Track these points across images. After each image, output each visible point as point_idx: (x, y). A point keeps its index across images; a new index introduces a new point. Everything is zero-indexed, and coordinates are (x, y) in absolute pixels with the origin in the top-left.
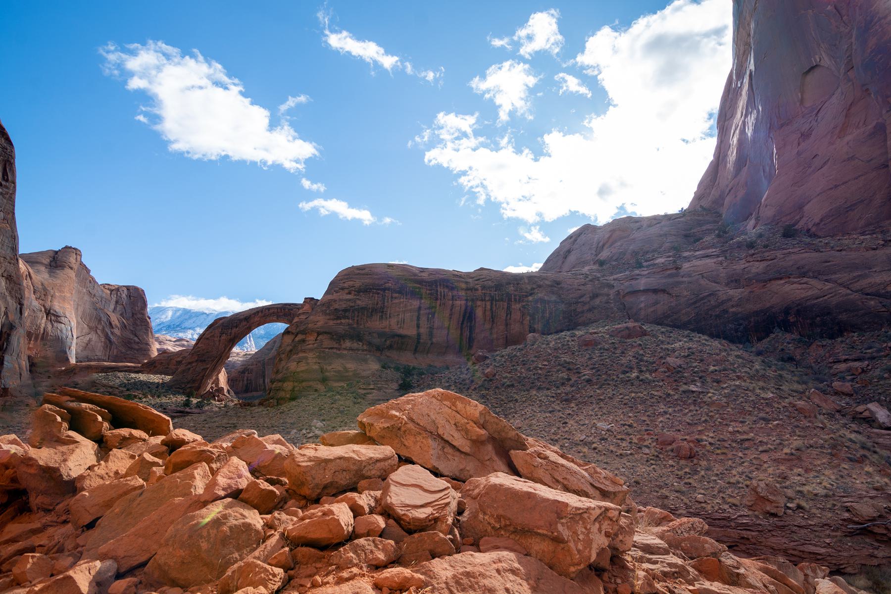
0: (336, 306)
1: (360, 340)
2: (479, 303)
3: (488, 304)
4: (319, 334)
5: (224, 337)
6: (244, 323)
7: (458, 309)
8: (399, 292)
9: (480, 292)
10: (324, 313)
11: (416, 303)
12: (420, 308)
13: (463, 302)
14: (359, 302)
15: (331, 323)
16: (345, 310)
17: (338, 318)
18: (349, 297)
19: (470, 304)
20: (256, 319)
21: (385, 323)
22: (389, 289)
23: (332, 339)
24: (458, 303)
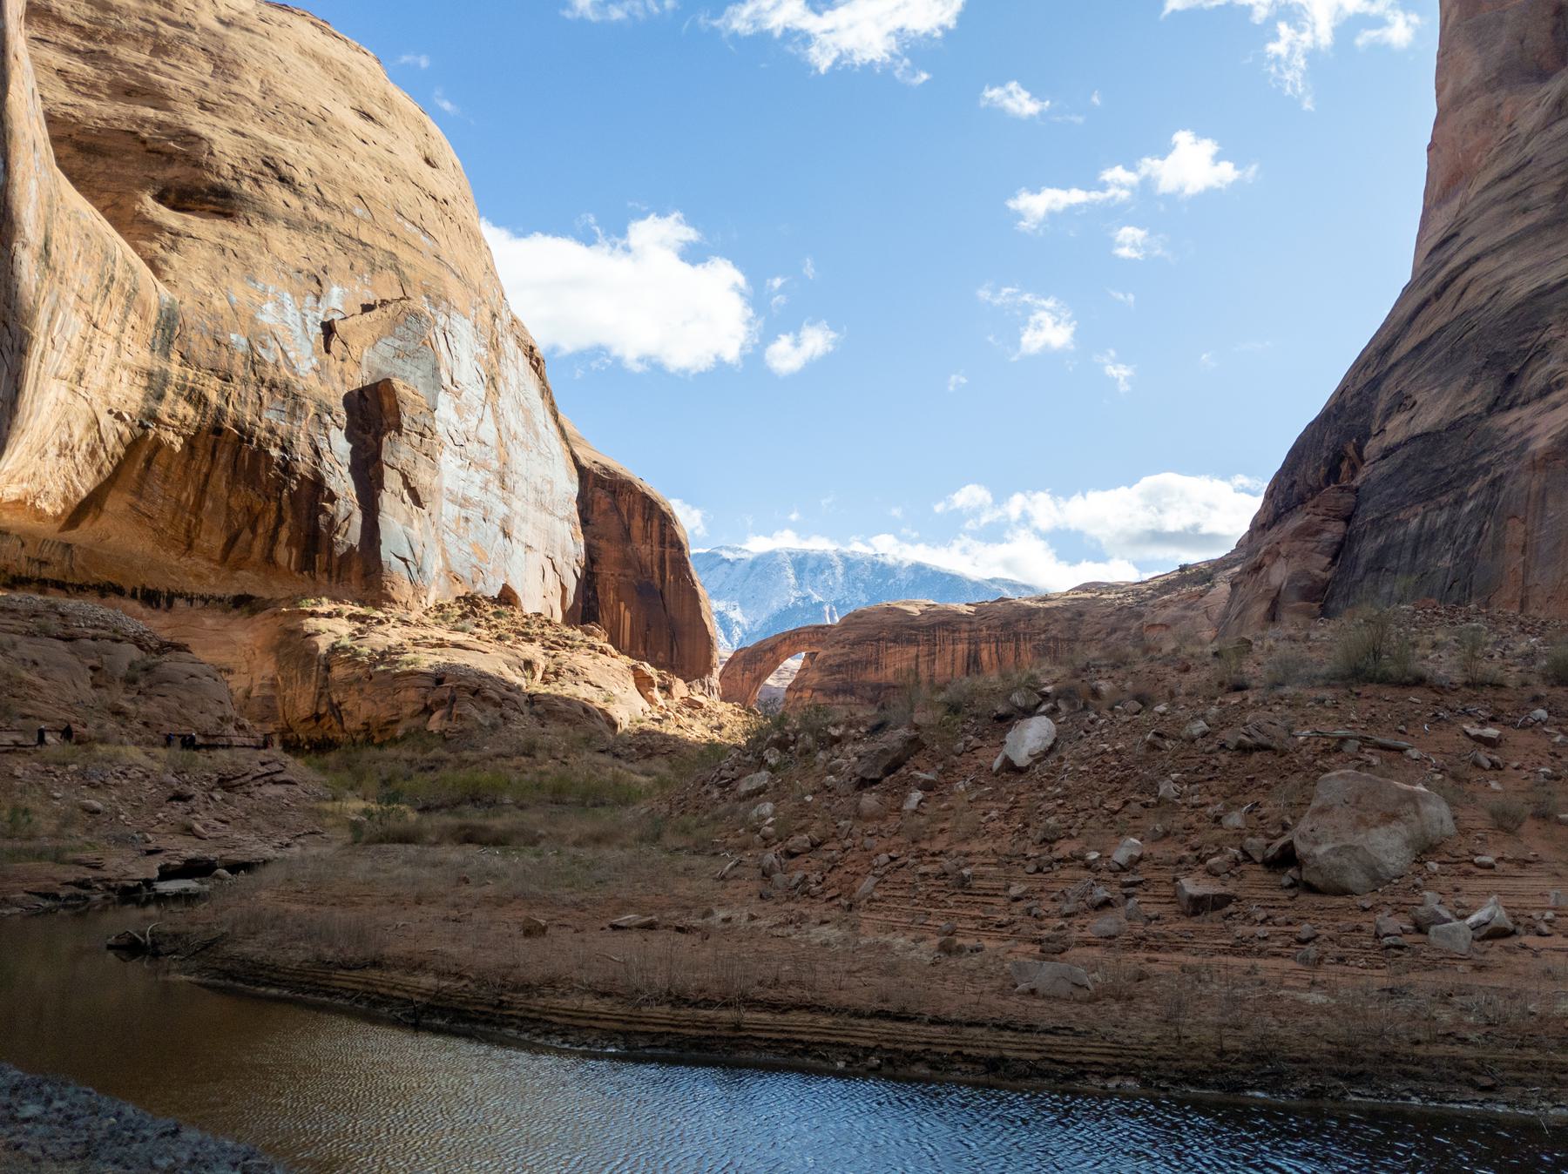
0: (830, 662)
1: (853, 694)
2: (983, 646)
3: (993, 646)
4: (814, 690)
5: (747, 674)
6: (769, 655)
7: (960, 653)
8: (894, 641)
9: (984, 633)
10: (820, 670)
11: (913, 651)
12: (917, 656)
13: (966, 646)
14: (853, 656)
15: (826, 679)
16: (839, 666)
17: (833, 674)
18: (843, 651)
19: (973, 647)
20: (785, 648)
21: (881, 674)
22: (883, 639)
23: (825, 695)
24: (960, 647)
